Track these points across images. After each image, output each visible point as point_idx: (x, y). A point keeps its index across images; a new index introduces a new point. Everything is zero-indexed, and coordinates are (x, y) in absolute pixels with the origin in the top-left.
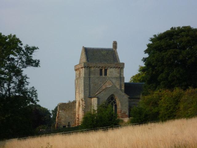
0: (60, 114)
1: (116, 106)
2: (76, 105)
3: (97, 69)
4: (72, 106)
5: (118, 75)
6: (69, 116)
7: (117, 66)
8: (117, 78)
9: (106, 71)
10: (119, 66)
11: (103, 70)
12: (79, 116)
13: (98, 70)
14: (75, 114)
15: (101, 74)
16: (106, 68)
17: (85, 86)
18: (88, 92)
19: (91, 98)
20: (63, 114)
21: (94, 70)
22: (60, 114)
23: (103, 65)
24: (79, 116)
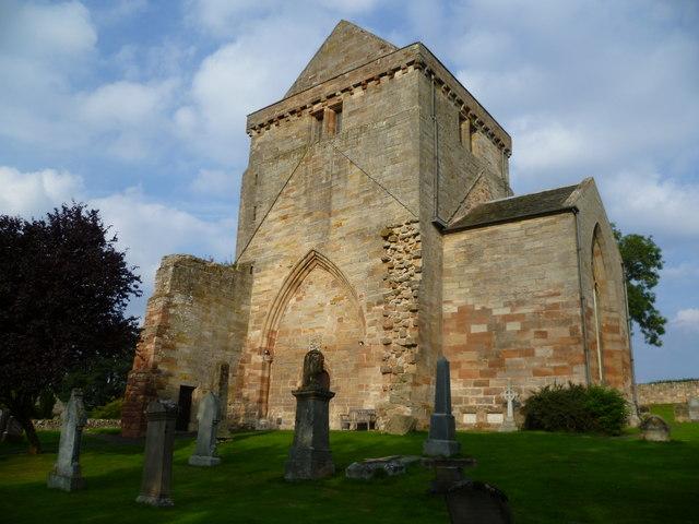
0: (172, 311)
2: (251, 285)
4: (234, 286)
12: (271, 342)
14: (242, 328)
17: (422, 157)
18: (430, 189)
19: (442, 230)
20: (187, 314)
22: (172, 311)
24: (271, 342)
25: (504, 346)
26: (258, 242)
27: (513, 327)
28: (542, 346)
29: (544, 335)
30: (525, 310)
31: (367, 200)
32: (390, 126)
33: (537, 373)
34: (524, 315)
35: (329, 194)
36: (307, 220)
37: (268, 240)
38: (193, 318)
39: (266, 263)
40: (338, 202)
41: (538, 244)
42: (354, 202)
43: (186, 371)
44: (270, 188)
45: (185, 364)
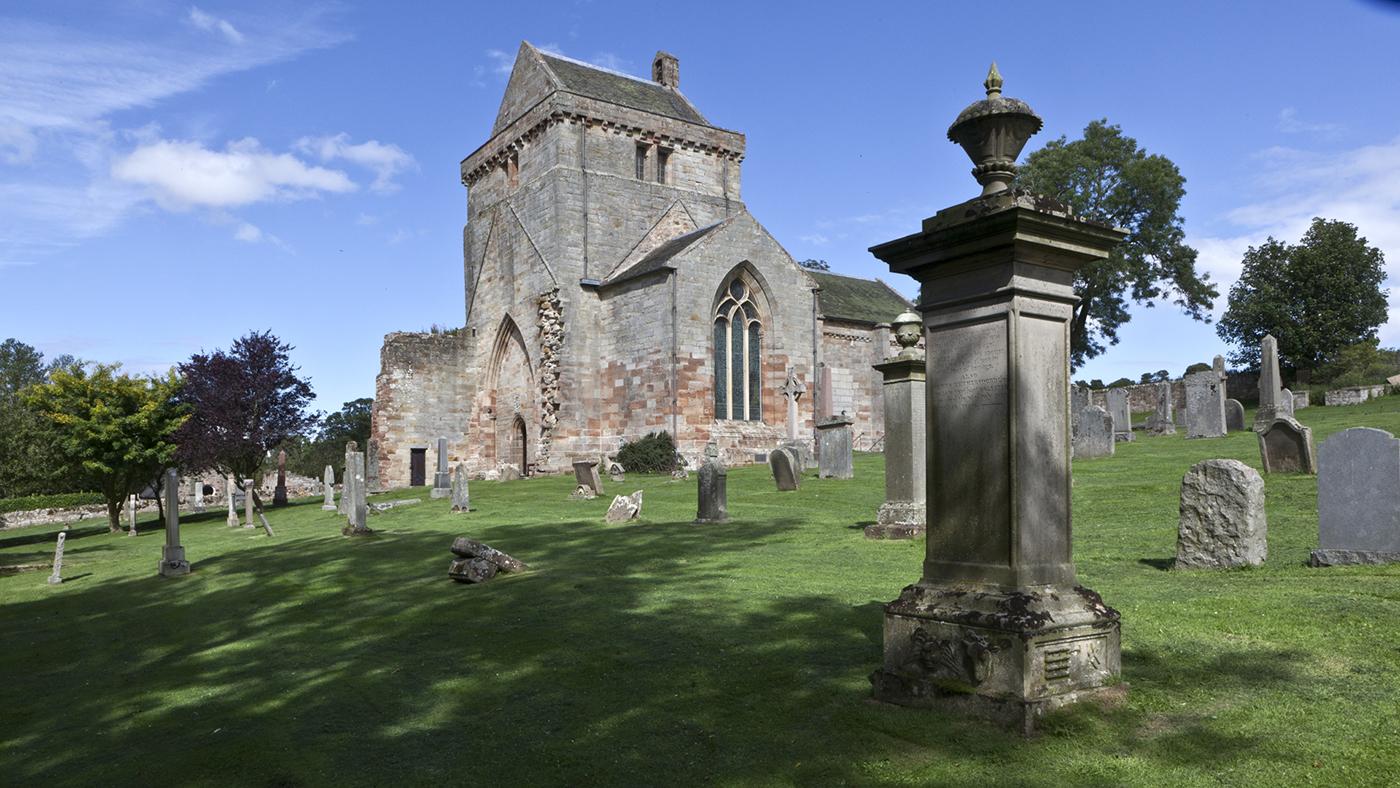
1: (754, 327)
3: (623, 135)
5: (719, 189)
6: (440, 400)
7: (713, 142)
8: (712, 201)
9: (663, 155)
10: (723, 146)
11: (651, 153)
13: (629, 141)
15: (640, 171)
16: (664, 144)
20: (409, 386)
21: (611, 143)
22: (393, 386)
23: (652, 123)
24: (493, 400)
25: (632, 399)
26: (477, 304)
27: (637, 381)
28: (651, 398)
29: (651, 388)
30: (643, 366)
31: (533, 265)
32: (543, 186)
33: (648, 423)
34: (641, 370)
35: (511, 259)
36: (502, 284)
37: (482, 302)
38: (416, 389)
39: (482, 325)
40: (518, 269)
41: (651, 303)
42: (526, 267)
43: (415, 436)
44: (478, 247)
45: (412, 429)
